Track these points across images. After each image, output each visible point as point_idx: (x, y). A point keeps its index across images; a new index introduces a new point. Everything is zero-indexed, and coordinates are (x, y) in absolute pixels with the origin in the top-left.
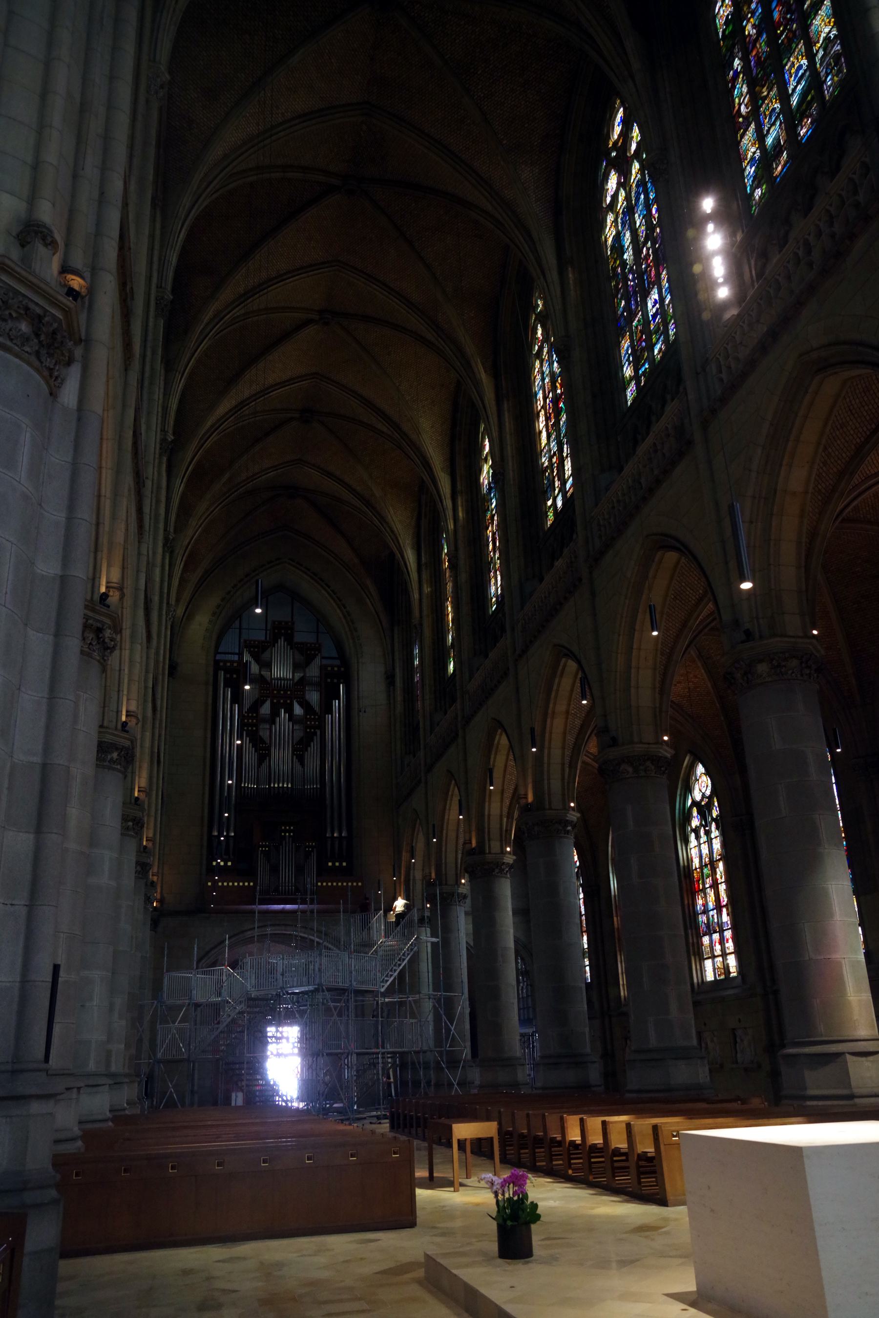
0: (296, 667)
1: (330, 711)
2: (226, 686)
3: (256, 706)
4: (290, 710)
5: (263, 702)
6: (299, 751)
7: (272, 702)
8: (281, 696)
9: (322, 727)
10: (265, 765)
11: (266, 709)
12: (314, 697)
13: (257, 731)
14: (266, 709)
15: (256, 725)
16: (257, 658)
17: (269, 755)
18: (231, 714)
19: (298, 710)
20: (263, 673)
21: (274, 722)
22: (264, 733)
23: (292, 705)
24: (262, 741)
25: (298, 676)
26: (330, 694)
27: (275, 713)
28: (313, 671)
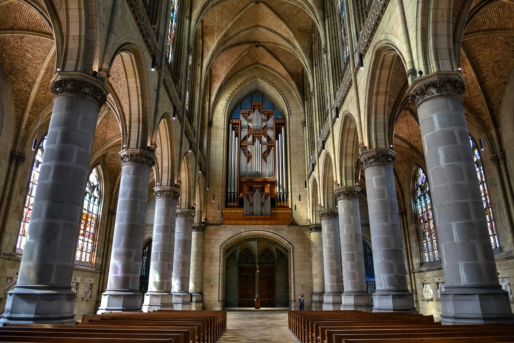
0: (263, 121)
1: (277, 138)
3: (245, 138)
4: (260, 139)
6: (264, 157)
8: (257, 134)
9: (274, 146)
11: (250, 139)
12: (271, 133)
14: (250, 139)
15: (246, 146)
17: (251, 158)
18: (235, 142)
19: (264, 139)
21: (253, 145)
22: (249, 149)
23: (261, 137)
25: (264, 124)
26: (278, 132)
27: (254, 141)
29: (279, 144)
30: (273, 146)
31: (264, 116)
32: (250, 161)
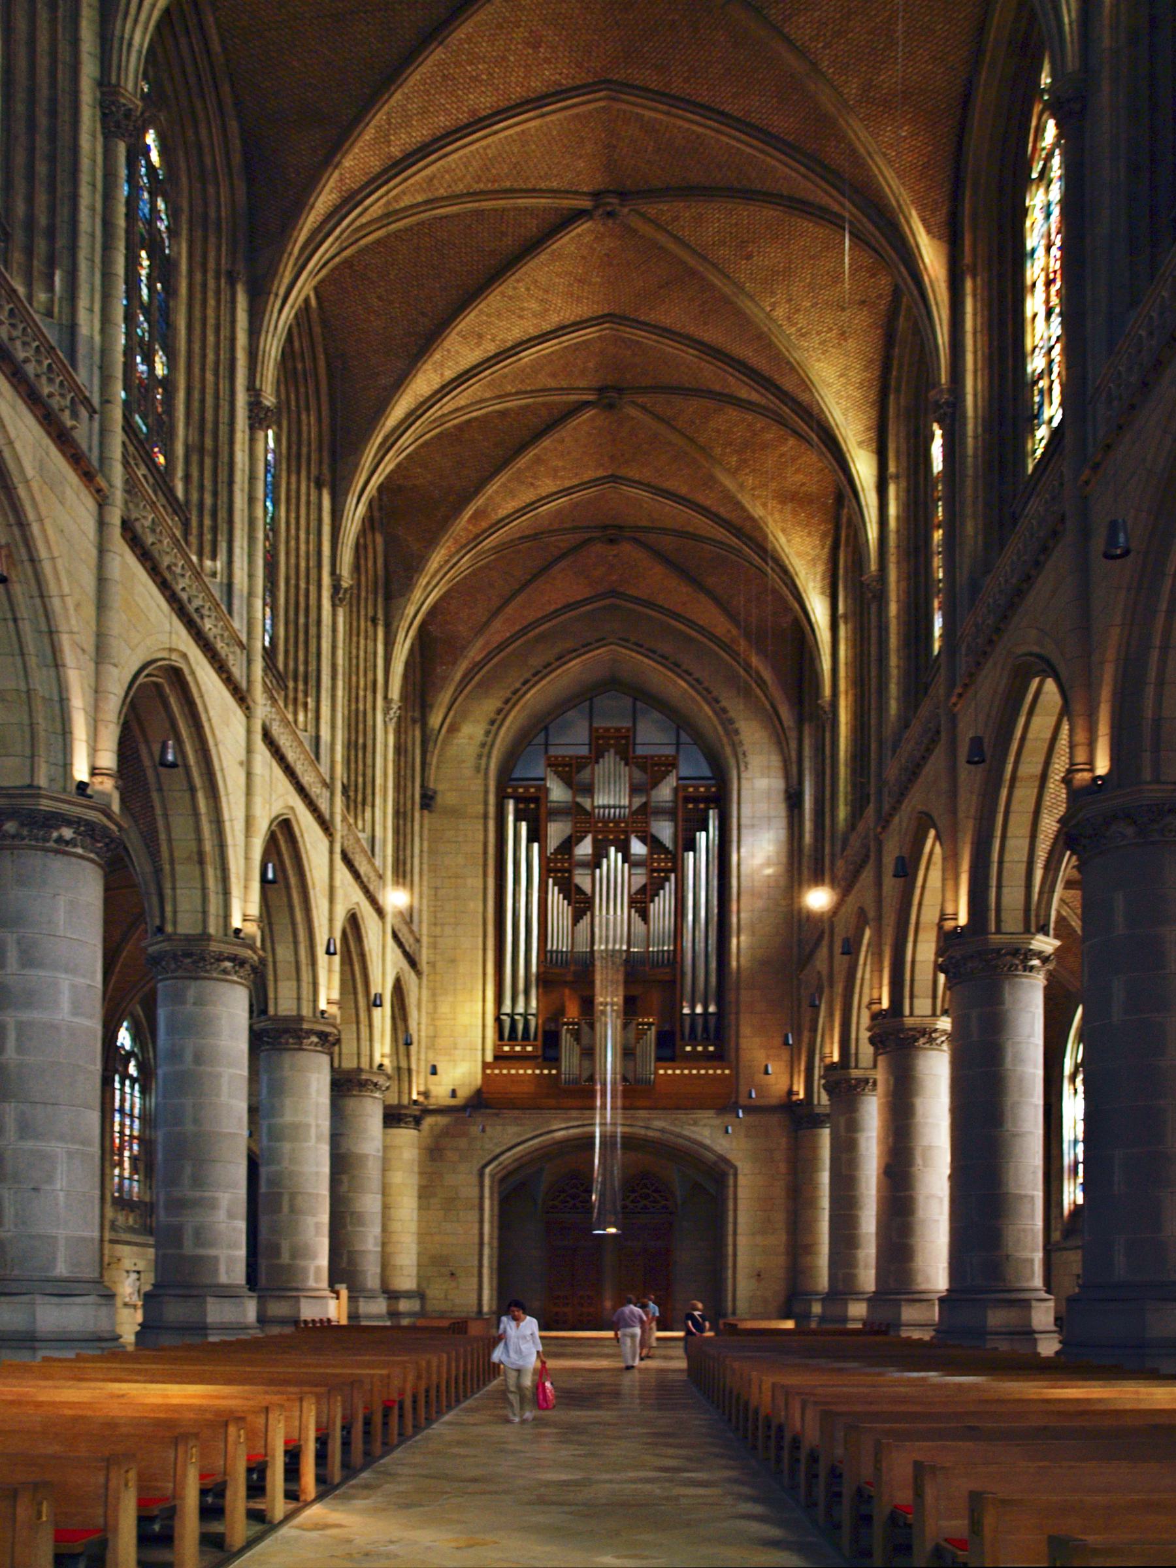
0: (634, 790)
1: (691, 846)
2: (517, 820)
3: (568, 845)
5: (580, 839)
6: (640, 902)
7: (595, 842)
10: (585, 922)
11: (585, 848)
12: (665, 831)
13: (570, 878)
14: (585, 848)
15: (569, 871)
16: (568, 782)
20: (579, 800)
21: (599, 866)
22: (582, 879)
24: (579, 890)
25: (638, 801)
28: (665, 792)
29: (698, 864)
30: (673, 870)
31: (638, 775)
32: (587, 919)
